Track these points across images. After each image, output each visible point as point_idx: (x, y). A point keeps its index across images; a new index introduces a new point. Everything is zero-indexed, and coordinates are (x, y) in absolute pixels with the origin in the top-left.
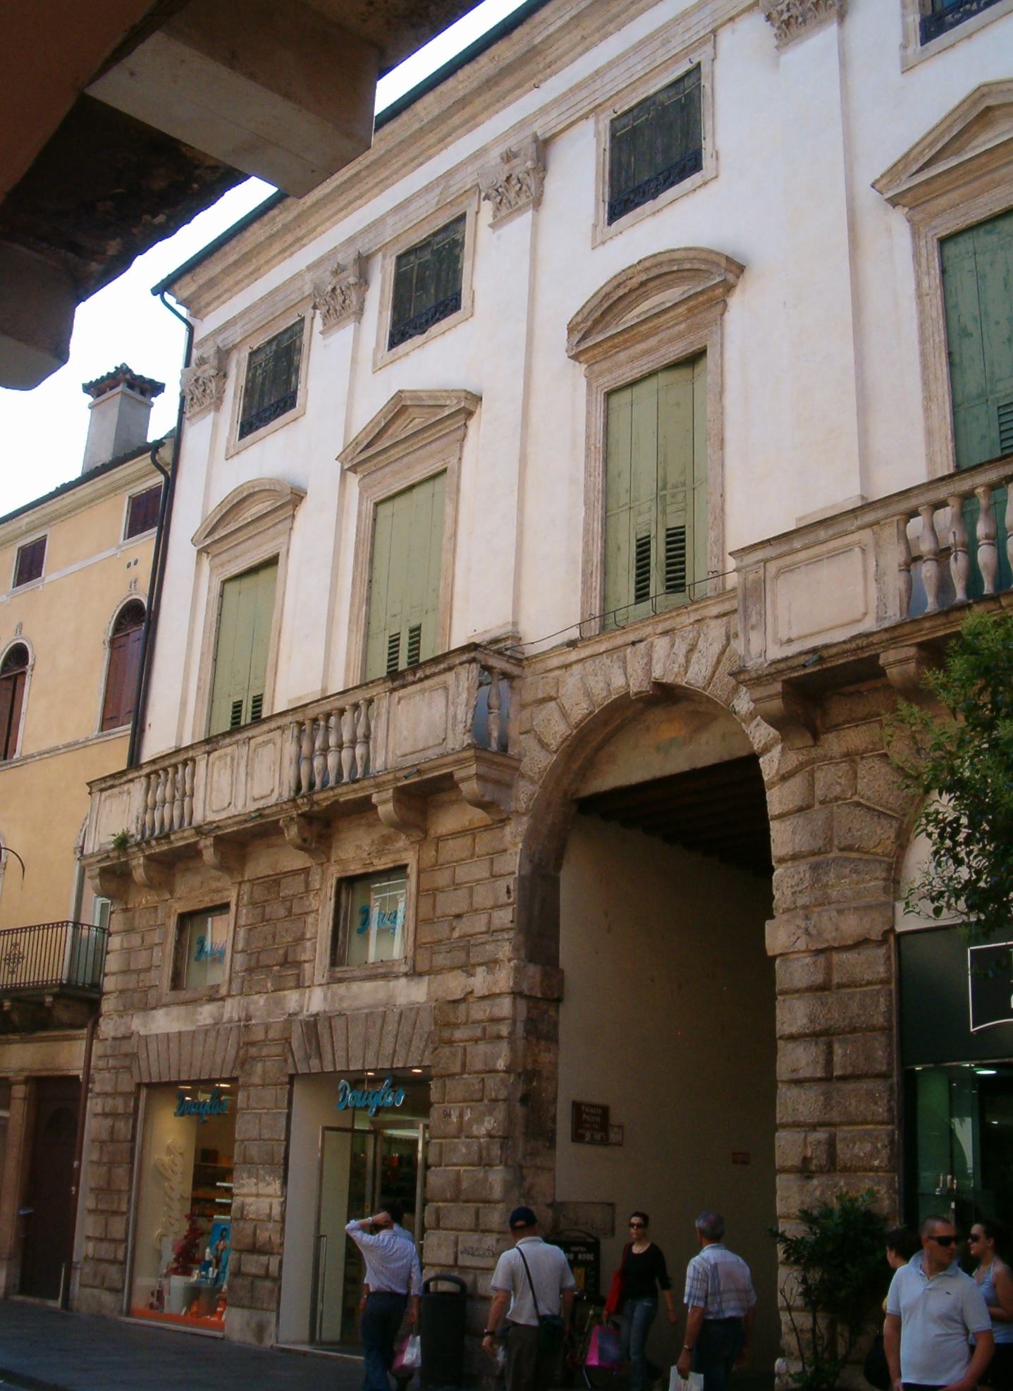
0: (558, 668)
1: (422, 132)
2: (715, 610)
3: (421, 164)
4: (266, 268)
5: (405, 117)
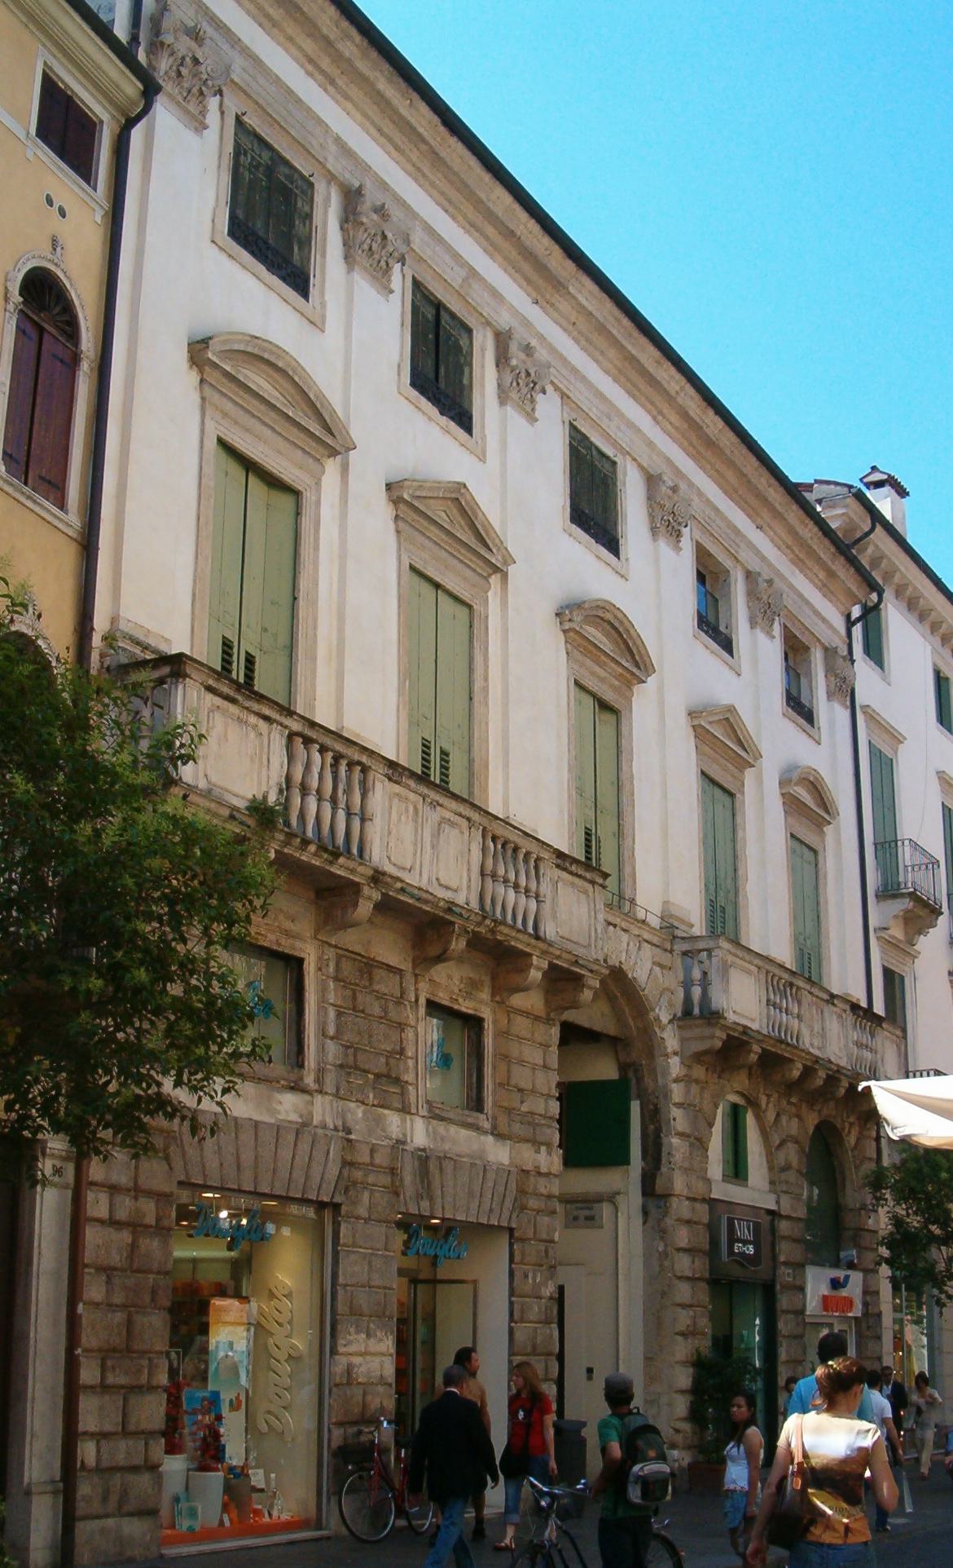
4: (282, 39)
5: (487, 177)
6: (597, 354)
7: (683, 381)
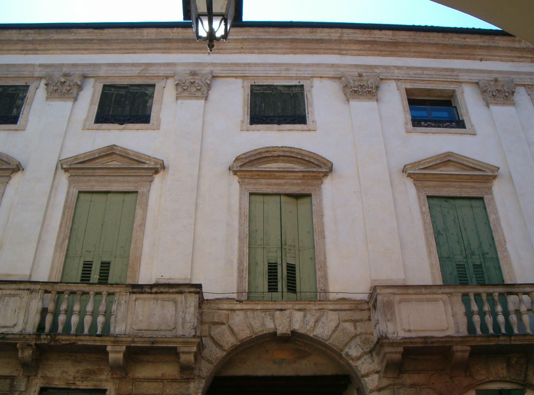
0: (227, 310)
1: (140, 41)
2: (331, 307)
3: (129, 53)
4: (6, 52)
5: (135, 31)
6: (270, 50)
7: (340, 30)
